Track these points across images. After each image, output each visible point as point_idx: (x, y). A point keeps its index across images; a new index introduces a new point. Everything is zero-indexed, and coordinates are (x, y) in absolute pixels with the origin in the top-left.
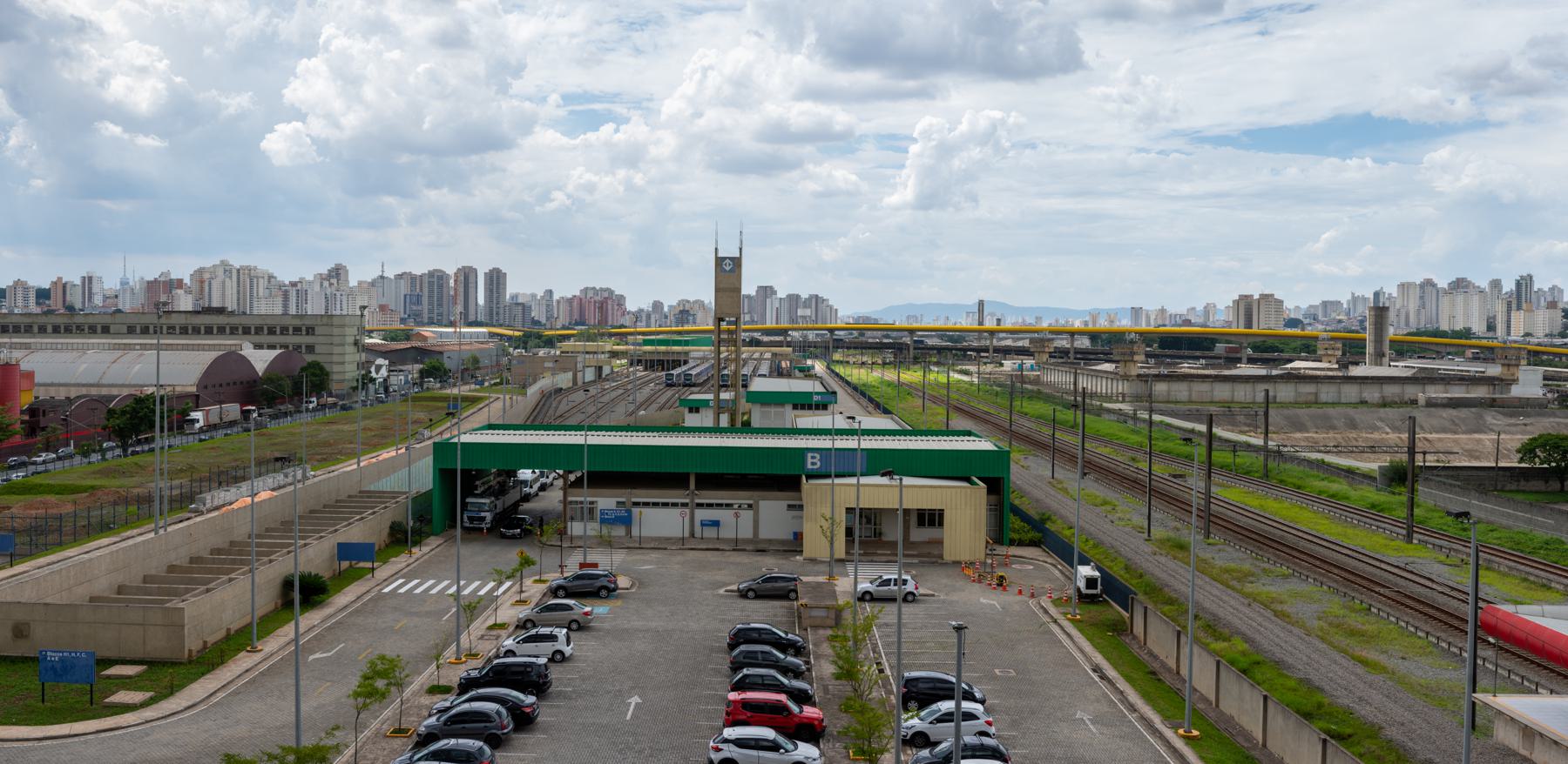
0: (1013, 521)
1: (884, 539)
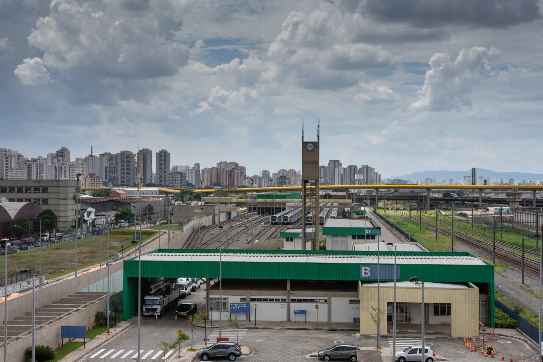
0: (498, 312)
1: (412, 322)
